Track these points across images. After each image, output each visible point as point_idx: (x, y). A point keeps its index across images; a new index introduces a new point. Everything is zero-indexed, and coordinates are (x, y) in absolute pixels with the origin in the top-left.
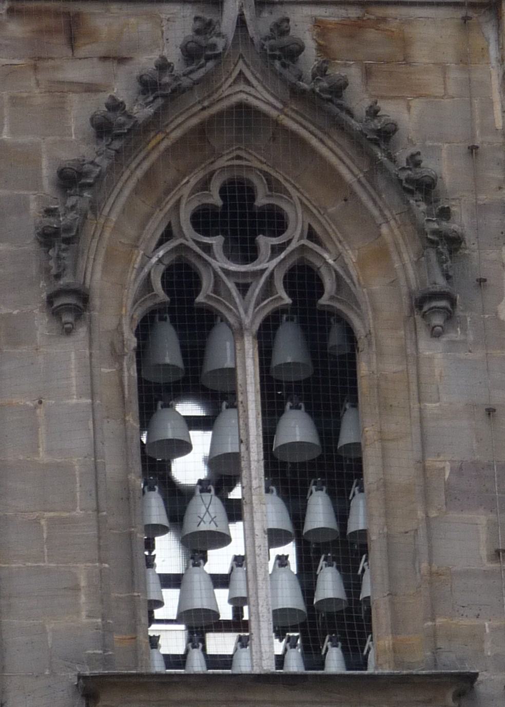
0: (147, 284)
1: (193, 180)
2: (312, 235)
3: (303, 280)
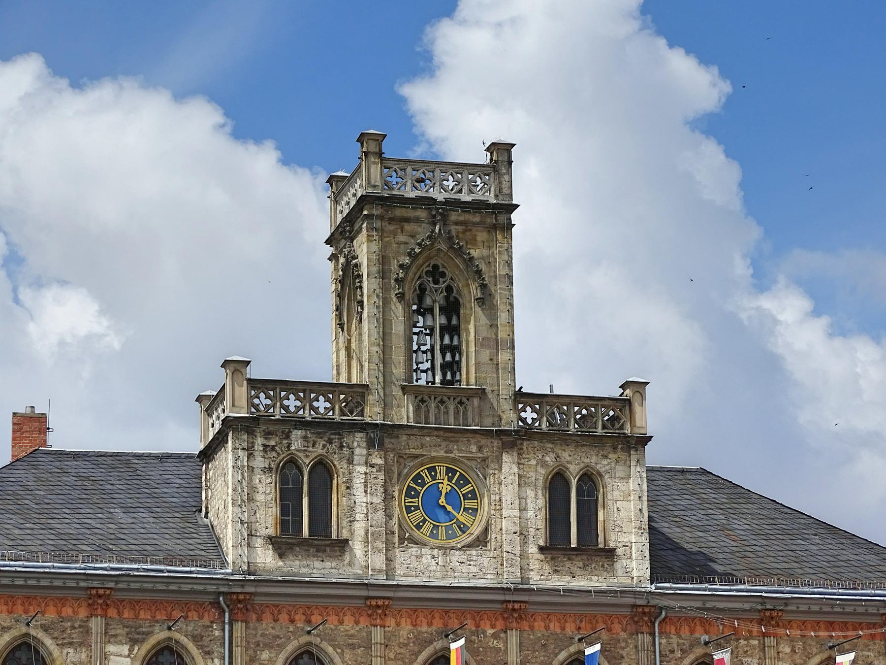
0: (415, 290)
1: (426, 264)
2: (452, 279)
3: (449, 289)
